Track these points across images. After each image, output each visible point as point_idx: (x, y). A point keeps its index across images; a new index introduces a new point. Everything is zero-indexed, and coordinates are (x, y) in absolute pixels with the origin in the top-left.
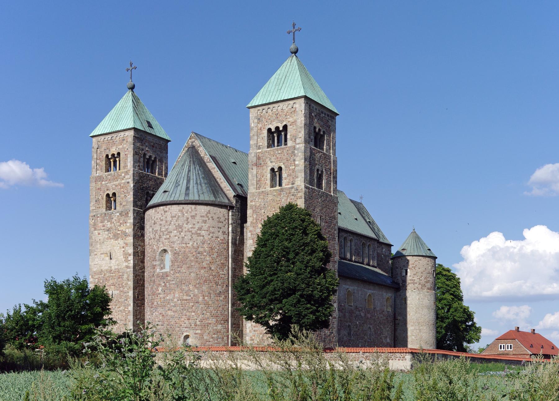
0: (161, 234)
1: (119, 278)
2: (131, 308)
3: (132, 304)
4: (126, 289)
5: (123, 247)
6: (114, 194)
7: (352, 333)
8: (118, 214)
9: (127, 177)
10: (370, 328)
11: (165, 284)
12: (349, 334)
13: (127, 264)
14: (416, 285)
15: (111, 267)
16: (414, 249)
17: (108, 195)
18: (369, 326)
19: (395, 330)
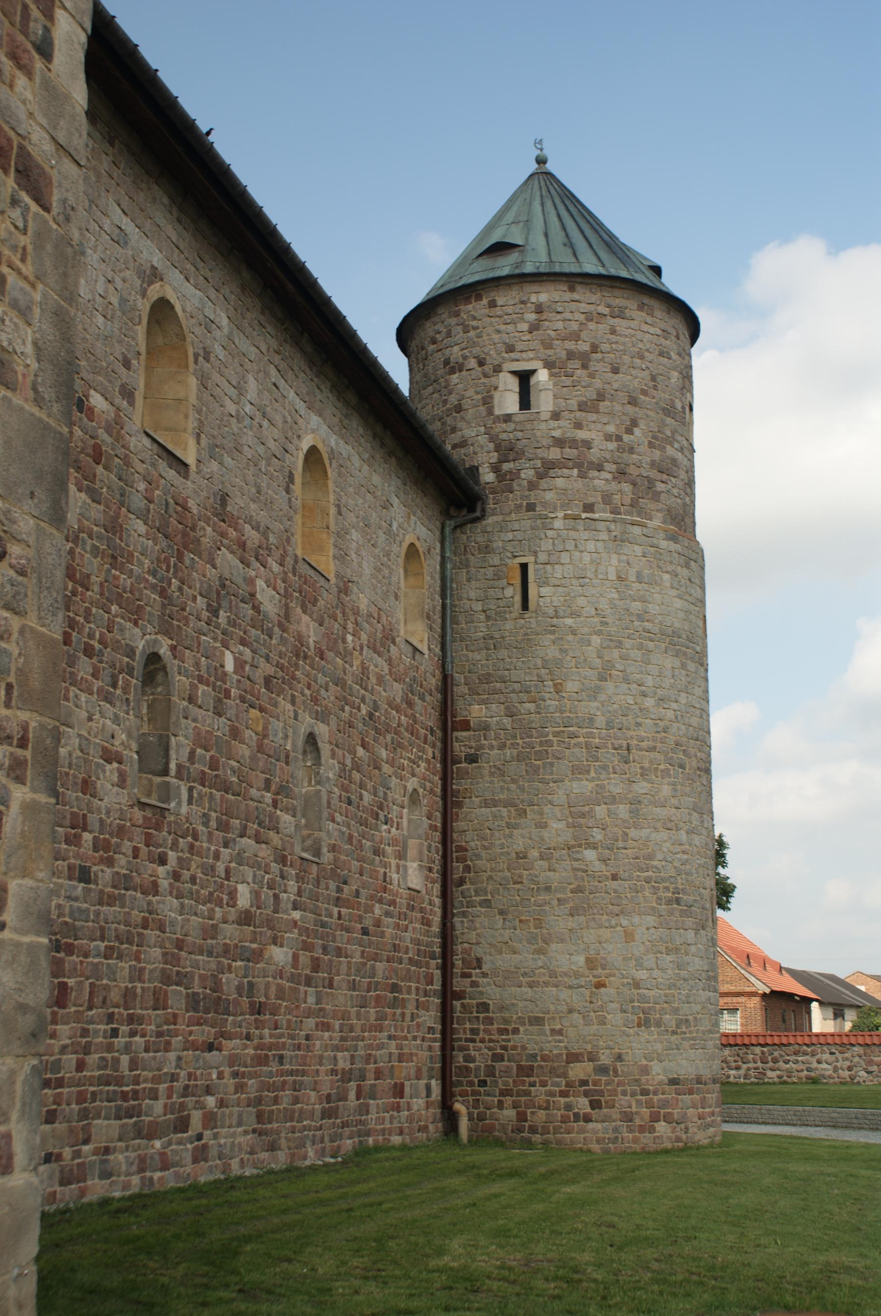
7: (180, 748)
10: (311, 739)
12: (154, 757)
14: (601, 481)
16: (569, 244)
18: (307, 722)
19: (449, 803)
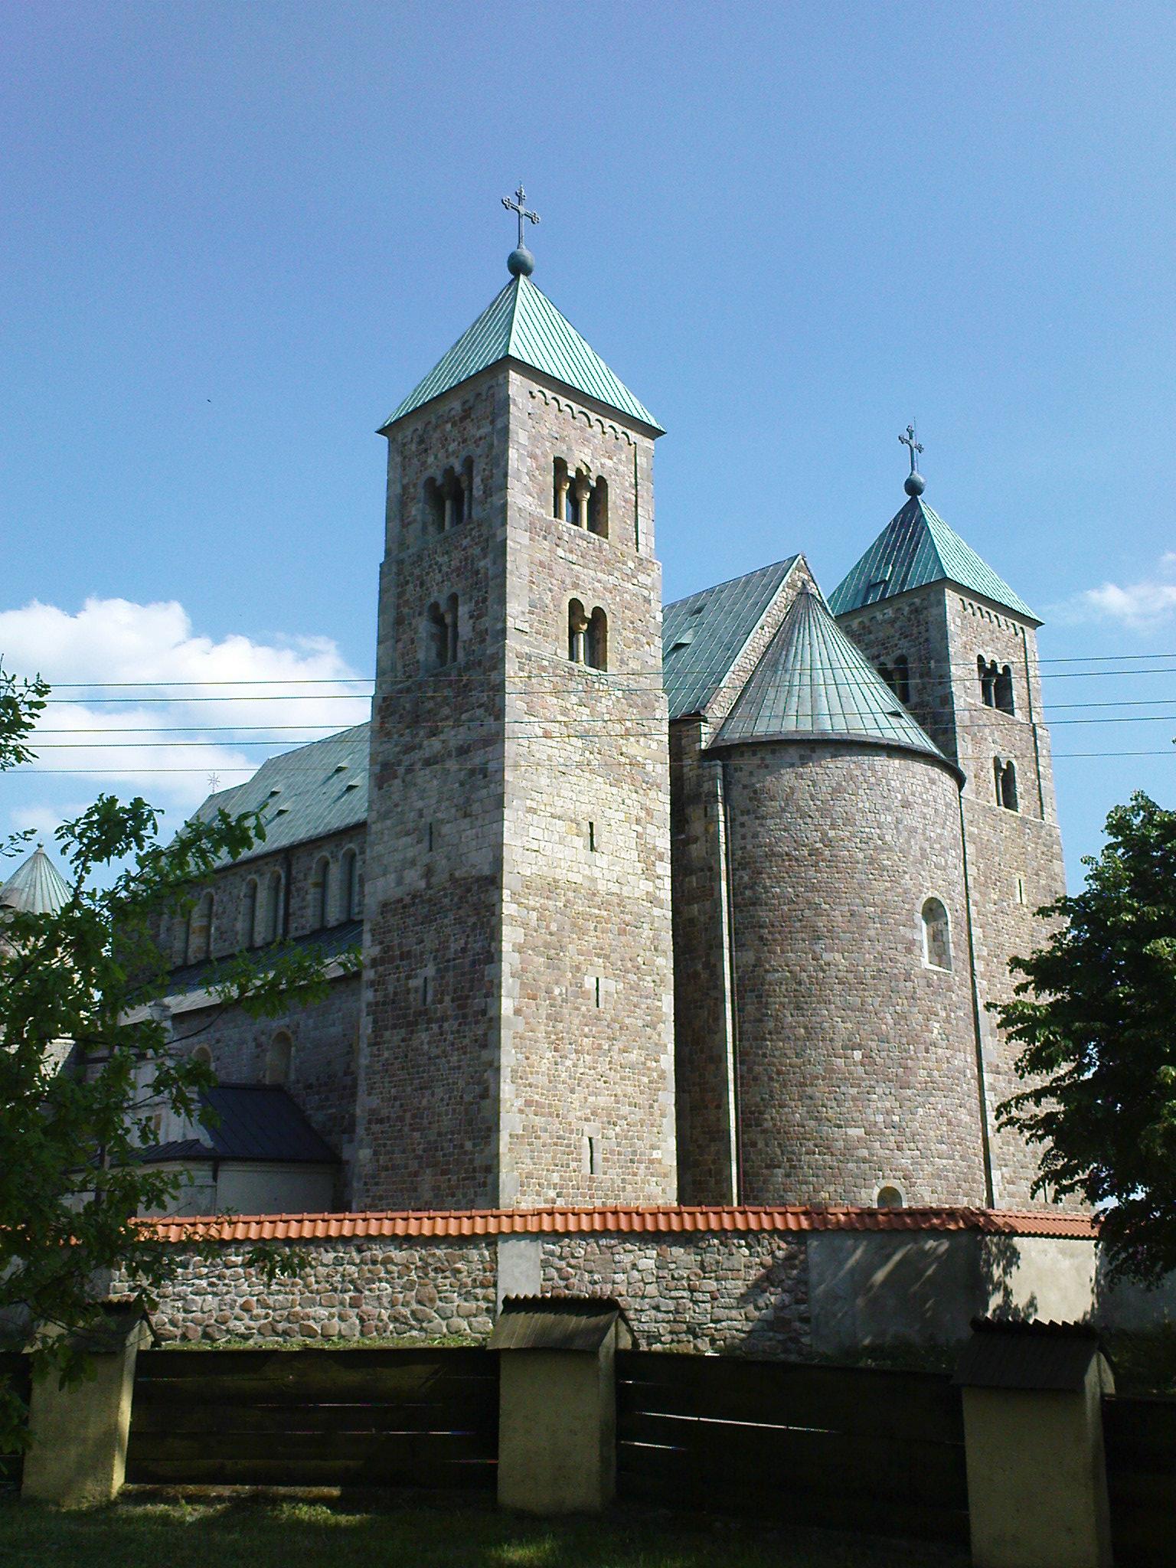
0: (926, 845)
1: (622, 932)
2: (668, 1061)
3: (671, 1048)
4: (648, 983)
5: (638, 822)
6: (598, 612)
8: (620, 694)
9: (642, 578)
11: (948, 1016)
13: (649, 886)
15: (594, 880)
17: (575, 606)
